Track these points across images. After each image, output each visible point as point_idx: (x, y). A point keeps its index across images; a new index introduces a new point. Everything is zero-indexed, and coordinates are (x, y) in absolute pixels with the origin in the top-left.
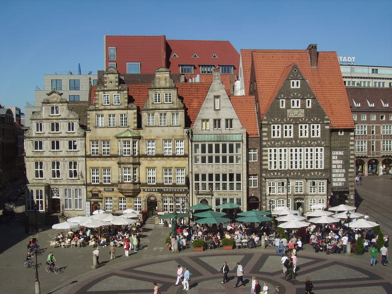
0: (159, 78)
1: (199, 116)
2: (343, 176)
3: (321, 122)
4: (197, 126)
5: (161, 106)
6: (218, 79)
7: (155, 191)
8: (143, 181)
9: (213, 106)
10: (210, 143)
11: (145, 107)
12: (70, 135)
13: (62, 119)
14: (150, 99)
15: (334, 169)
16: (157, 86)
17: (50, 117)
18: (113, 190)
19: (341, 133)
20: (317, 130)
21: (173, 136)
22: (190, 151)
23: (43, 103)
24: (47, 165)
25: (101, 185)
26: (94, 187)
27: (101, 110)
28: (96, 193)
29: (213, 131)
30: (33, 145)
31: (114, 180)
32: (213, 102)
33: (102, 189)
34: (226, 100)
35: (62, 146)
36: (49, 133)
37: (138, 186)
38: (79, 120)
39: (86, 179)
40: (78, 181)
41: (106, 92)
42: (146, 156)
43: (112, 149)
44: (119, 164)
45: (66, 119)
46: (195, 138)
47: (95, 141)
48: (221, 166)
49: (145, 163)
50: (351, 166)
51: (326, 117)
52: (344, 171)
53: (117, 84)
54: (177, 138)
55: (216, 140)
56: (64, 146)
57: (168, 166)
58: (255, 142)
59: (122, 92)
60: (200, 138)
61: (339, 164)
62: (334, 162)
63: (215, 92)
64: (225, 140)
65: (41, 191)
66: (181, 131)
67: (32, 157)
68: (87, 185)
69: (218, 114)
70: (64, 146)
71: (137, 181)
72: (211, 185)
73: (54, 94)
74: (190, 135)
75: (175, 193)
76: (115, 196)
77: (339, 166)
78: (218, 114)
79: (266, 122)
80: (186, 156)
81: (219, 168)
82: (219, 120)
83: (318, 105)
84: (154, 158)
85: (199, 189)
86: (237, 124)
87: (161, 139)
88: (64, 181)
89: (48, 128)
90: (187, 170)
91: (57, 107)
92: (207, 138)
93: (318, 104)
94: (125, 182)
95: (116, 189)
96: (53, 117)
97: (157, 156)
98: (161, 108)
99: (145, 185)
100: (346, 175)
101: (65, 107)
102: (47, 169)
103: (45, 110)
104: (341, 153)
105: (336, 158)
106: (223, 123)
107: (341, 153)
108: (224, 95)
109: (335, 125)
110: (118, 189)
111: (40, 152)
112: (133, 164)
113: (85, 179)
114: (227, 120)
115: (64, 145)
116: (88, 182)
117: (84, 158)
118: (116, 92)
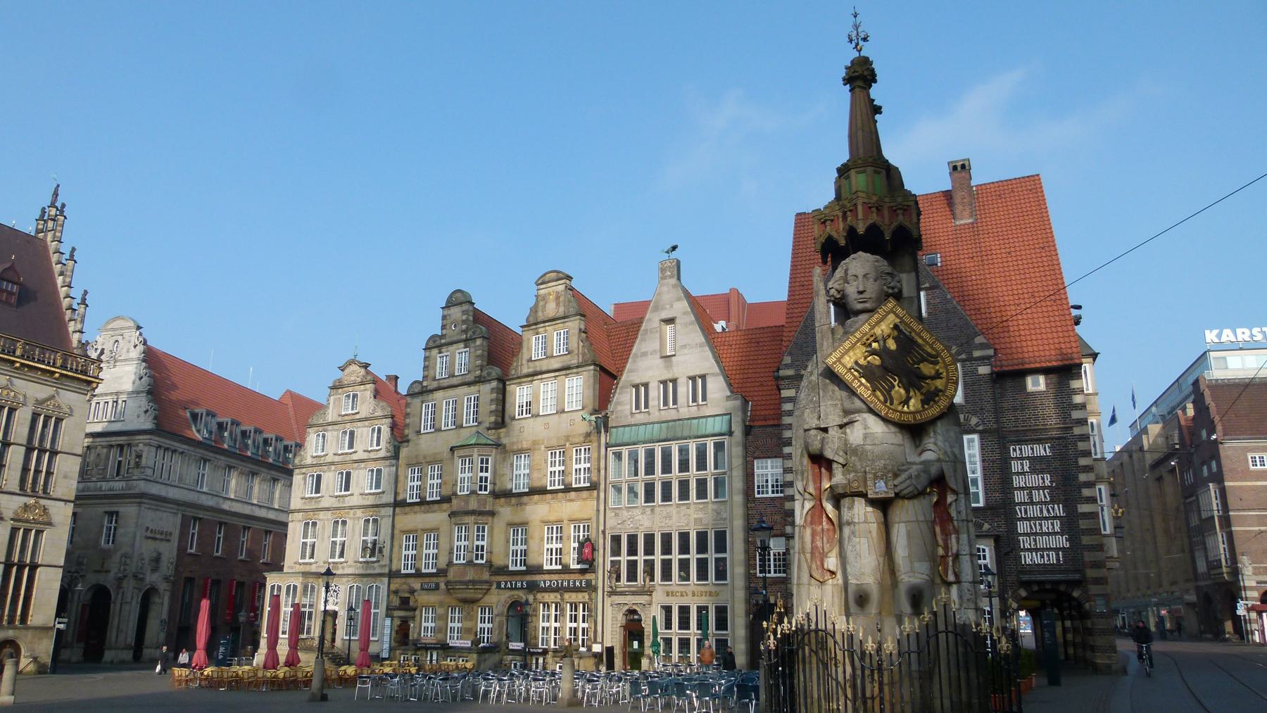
0: (544, 298)
1: (624, 378)
2: (1057, 529)
3: (963, 356)
4: (623, 401)
5: (544, 366)
6: (671, 277)
7: (522, 588)
8: (498, 561)
9: (656, 345)
10: (649, 446)
11: (513, 372)
12: (373, 455)
13: (360, 420)
14: (525, 350)
15: (1021, 504)
16: (541, 316)
17: (340, 419)
18: (437, 587)
19: (1036, 383)
21: (567, 438)
22: (602, 472)
23: (331, 388)
24: (323, 528)
25: (418, 574)
26: (403, 580)
27: (432, 391)
28: (407, 595)
29: (657, 413)
30: (305, 484)
31: (442, 563)
32: (658, 335)
34: (691, 327)
35: (354, 484)
36: (335, 454)
37: (486, 576)
38: (393, 417)
39: (391, 561)
40: (376, 565)
41: (444, 350)
42: (508, 494)
43: (445, 483)
44: (452, 515)
45: (366, 419)
46: (616, 435)
48: (673, 511)
49: (506, 512)
50: (1086, 492)
51: (979, 340)
52: (1059, 510)
53: (464, 327)
54: (577, 440)
55: (663, 436)
56: (357, 483)
57: (552, 518)
59: (473, 345)
60: (626, 435)
61: (1038, 488)
62: (1017, 481)
63: (663, 309)
64: (686, 434)
65: (295, 587)
66: (581, 424)
67: (299, 511)
68: (393, 575)
69: (669, 366)
70: (357, 483)
71: (484, 562)
72: (650, 565)
73: (354, 368)
74: (603, 424)
75: (559, 589)
76: (441, 604)
77: (1037, 496)
78: (671, 366)
79: (790, 372)
80: (594, 487)
81: (669, 517)
82: (674, 381)
83: (949, 306)
84: (525, 499)
85: (618, 579)
86: (717, 388)
87: (543, 448)
88: (350, 566)
89: (334, 443)
90: (595, 526)
91: (355, 396)
92: (642, 432)
93: (948, 301)
94: (458, 562)
95: (442, 586)
96: (346, 418)
98: (544, 369)
99: (503, 571)
100: (1070, 525)
101: (369, 392)
102: (323, 539)
103: (334, 403)
104: (1041, 450)
105: (1026, 469)
106: (684, 389)
107: (1041, 450)
108: (685, 313)
110: (447, 584)
111: (313, 498)
112: (473, 513)
113: (388, 563)
114: (693, 379)
116: (394, 568)
117: (392, 509)
118: (462, 345)
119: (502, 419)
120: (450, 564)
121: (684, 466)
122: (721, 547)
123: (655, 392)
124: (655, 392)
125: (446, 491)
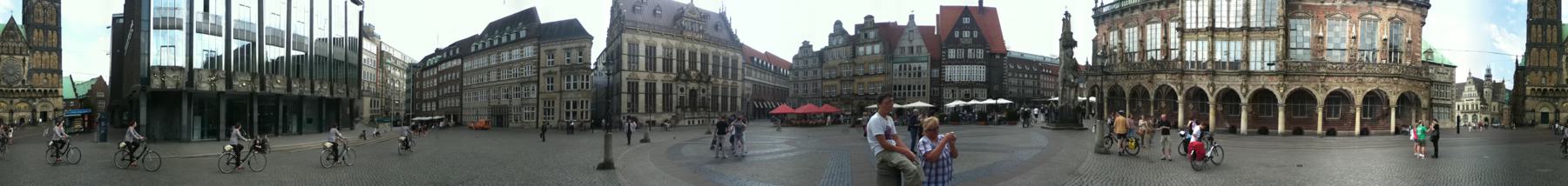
20: (980, 53)
31: (839, 93)
33: (831, 100)
42: (857, 76)
44: (841, 81)
46: (896, 60)
47: (830, 68)
49: (857, 80)
58: (938, 62)
60: (898, 60)
68: (823, 97)
72: (904, 94)
82: (912, 48)
86: (924, 50)
97: (865, 75)
99: (857, 95)
106: (915, 50)
109: (994, 50)
114: (918, 47)
115: (811, 73)
119: (854, 55)
120: (841, 94)
121: (905, 69)
122: (924, 88)
123: (906, 49)
124: (906, 49)
125: (839, 75)
